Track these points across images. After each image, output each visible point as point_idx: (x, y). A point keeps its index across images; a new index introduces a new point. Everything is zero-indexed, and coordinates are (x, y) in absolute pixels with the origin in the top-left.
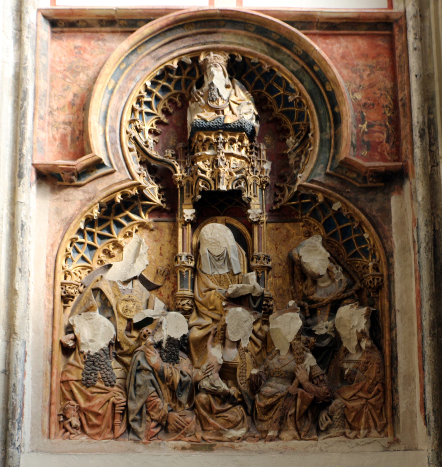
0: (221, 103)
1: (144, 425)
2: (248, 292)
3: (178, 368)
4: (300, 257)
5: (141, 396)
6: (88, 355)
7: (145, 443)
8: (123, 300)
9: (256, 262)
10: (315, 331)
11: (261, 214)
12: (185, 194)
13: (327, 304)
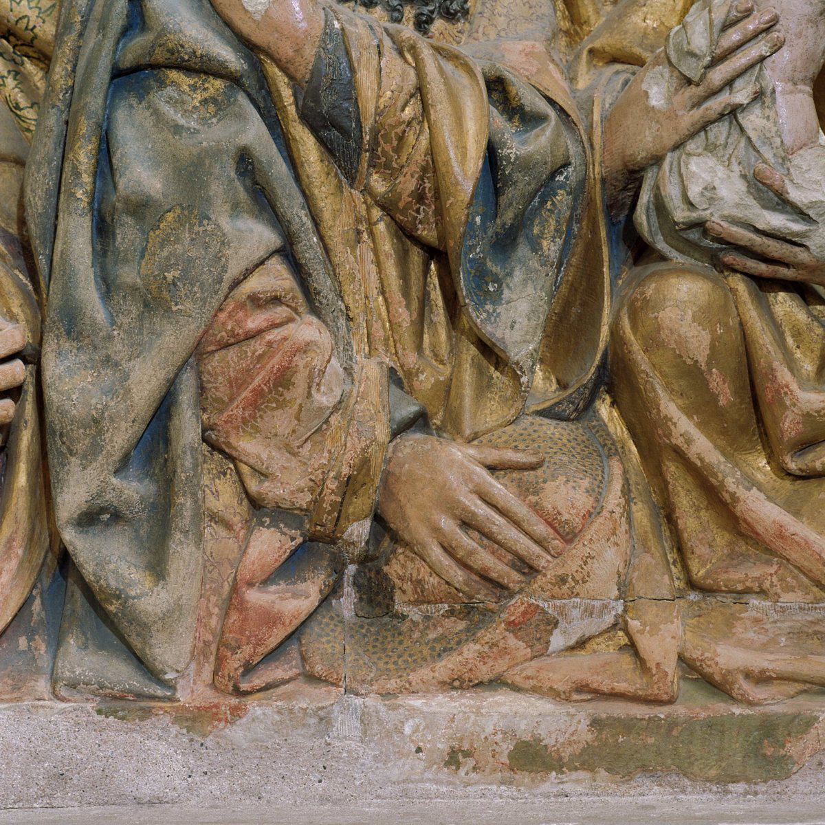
3: (464, 50)
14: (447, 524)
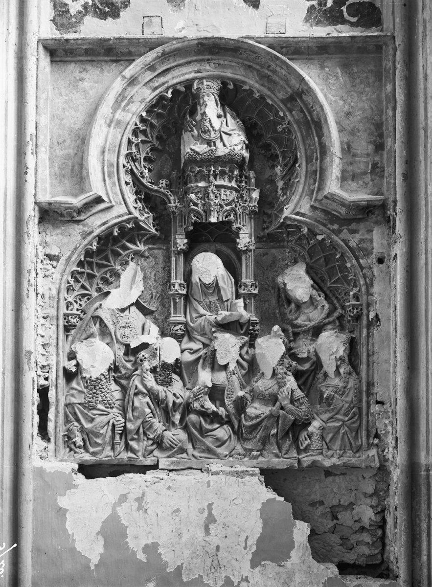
0: (213, 135)
4: (285, 285)
5: (137, 418)
6: (90, 380)
9: (244, 290)
13: (309, 330)
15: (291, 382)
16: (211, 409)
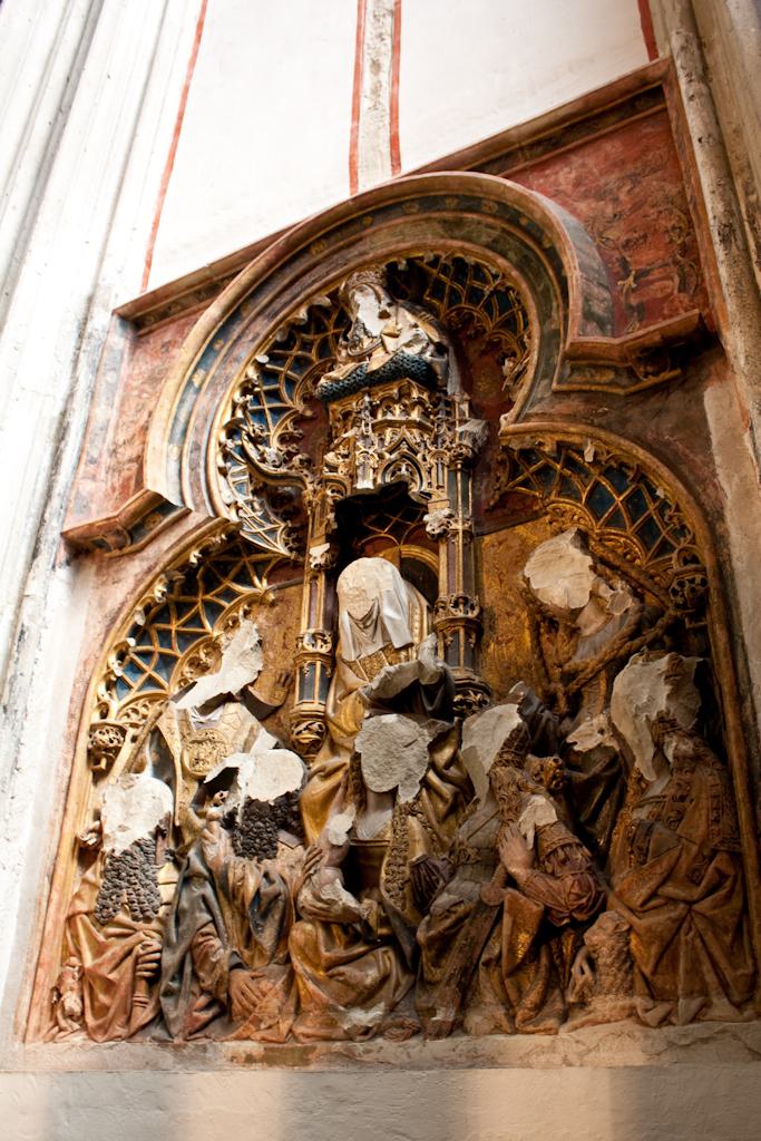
1: (182, 1003)
2: (408, 680)
6: (112, 857)
7: (177, 1047)
8: (193, 742)
10: (575, 743)
11: (450, 516)
12: (317, 522)
13: (596, 675)
14: (239, 994)
15: (541, 811)
16: (340, 903)
